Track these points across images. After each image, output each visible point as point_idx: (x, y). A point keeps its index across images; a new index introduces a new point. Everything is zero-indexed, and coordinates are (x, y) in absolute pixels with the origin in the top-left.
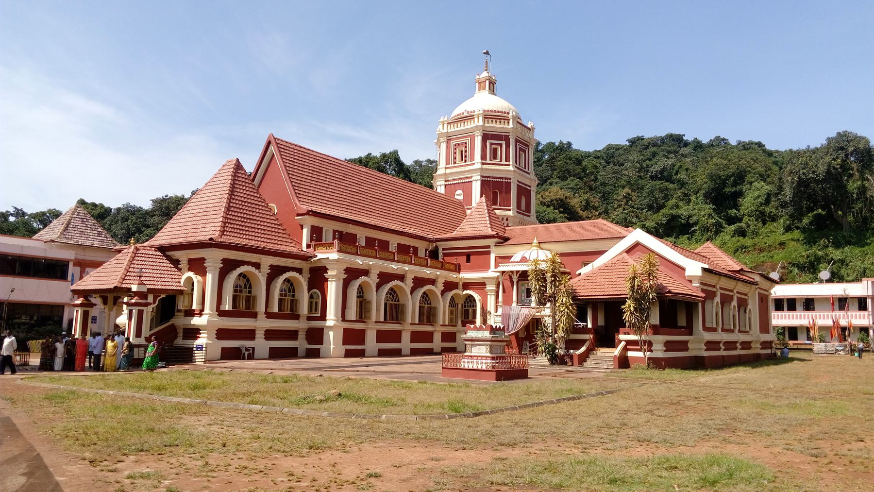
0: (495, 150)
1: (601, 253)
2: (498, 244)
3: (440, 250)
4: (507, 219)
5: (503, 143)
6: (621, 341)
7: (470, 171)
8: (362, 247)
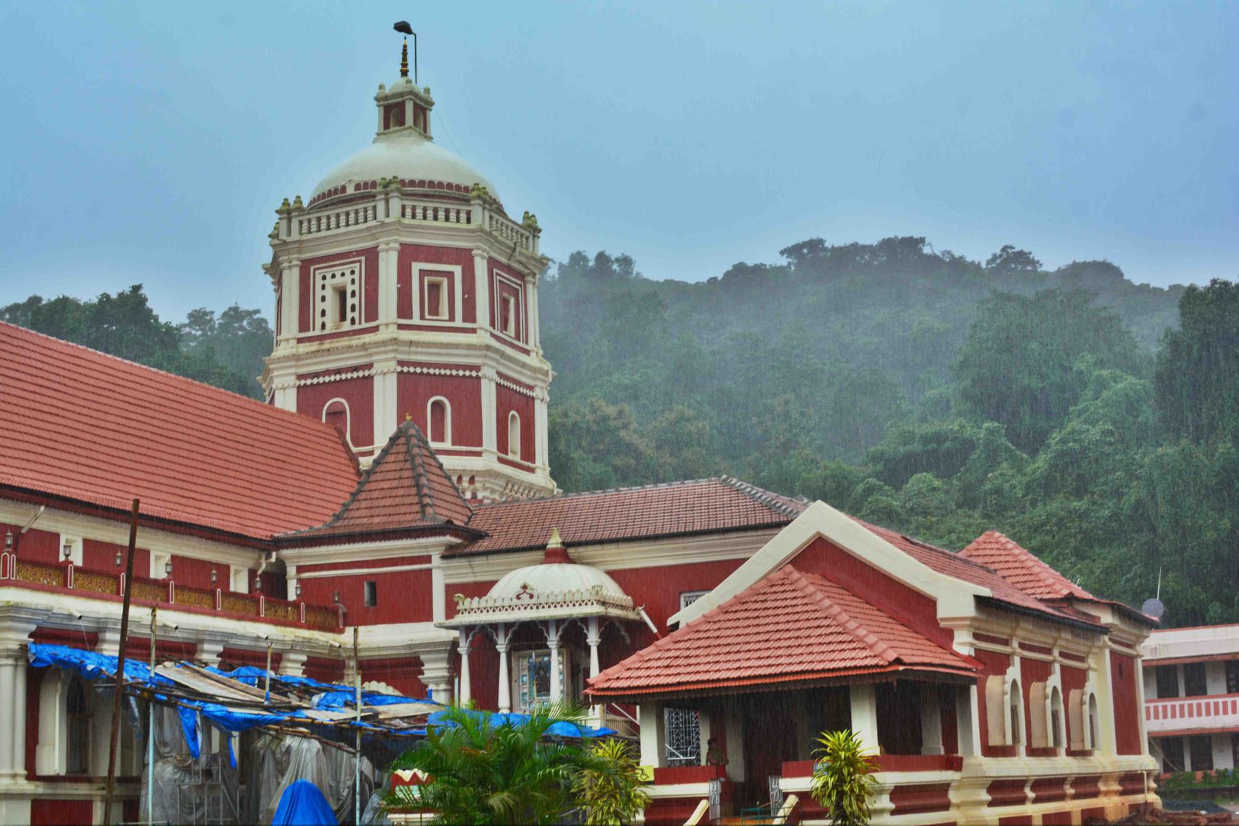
0: (434, 287)
1: (728, 568)
2: (450, 554)
3: (291, 571)
4: (472, 481)
5: (457, 270)
6: (785, 795)
7: (364, 347)
8: (77, 569)
